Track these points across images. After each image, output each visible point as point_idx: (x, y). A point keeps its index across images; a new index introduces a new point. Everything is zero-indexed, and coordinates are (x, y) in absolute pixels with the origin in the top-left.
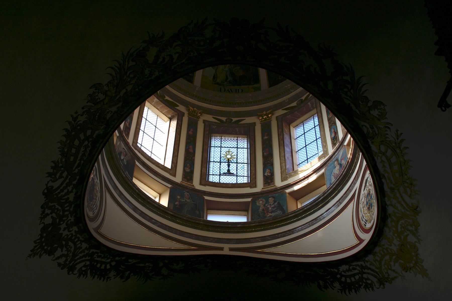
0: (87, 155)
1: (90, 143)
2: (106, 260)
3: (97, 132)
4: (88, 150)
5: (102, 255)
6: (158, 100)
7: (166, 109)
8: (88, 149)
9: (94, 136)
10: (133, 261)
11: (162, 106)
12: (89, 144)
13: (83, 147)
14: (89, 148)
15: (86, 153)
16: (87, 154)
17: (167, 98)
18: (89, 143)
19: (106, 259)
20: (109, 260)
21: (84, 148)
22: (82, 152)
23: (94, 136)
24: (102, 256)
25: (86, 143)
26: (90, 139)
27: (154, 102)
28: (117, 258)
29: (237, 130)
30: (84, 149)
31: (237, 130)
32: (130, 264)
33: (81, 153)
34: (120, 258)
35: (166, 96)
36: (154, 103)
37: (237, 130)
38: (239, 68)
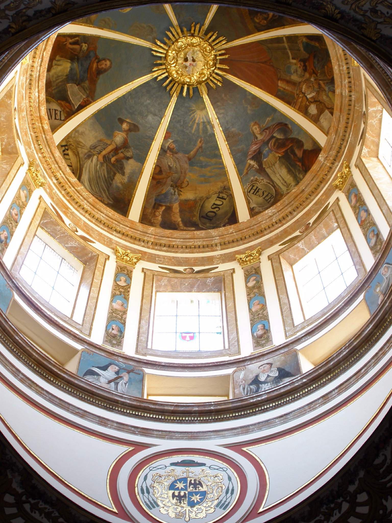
0: (51, 510)
1: (30, 500)
2: (340, 512)
3: (14, 485)
4: (42, 505)
5: (318, 518)
6: (303, 241)
7: (320, 230)
8: (41, 505)
9: (20, 491)
10: (383, 455)
11: (315, 236)
12: (33, 502)
13: (32, 512)
14: (41, 503)
15: (47, 511)
16: (49, 509)
17: (311, 221)
18: (29, 502)
19: (336, 511)
20: (345, 506)
21: (35, 513)
22: (41, 515)
23: (20, 491)
24: (323, 518)
25: (27, 507)
26: (24, 498)
27: (303, 249)
28: (352, 488)
29: (373, 109)
30: (37, 512)
31: (375, 109)
32: (388, 461)
33: (42, 518)
34: (357, 483)
35: (309, 222)
36: (306, 249)
37: (375, 109)
38: (326, 67)
